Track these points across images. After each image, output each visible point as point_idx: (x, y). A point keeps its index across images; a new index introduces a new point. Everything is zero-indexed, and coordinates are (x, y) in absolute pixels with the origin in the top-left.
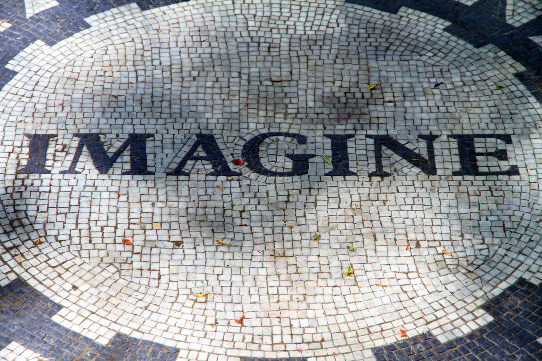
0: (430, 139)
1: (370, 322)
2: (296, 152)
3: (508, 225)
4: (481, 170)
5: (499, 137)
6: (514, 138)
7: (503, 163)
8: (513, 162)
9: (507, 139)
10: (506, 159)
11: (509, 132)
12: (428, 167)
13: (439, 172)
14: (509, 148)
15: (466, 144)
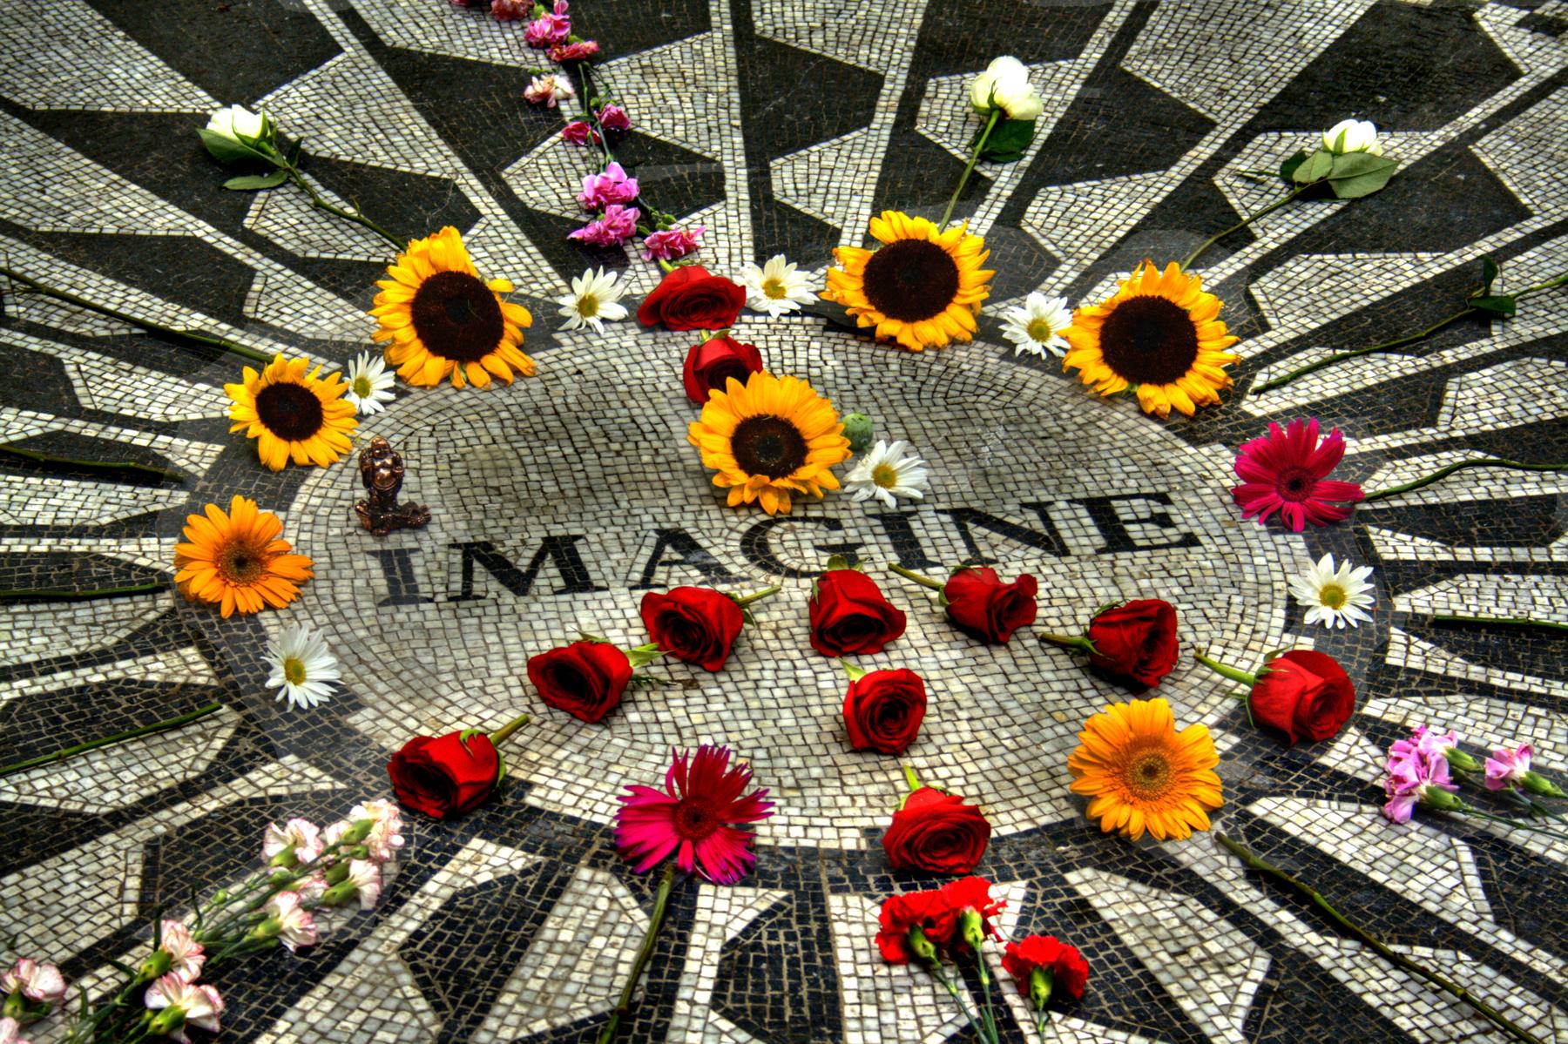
0: (1041, 508)
1: (1047, 761)
2: (832, 541)
3: (1211, 613)
4: (1139, 543)
5: (1147, 496)
6: (1173, 496)
7: (1169, 531)
8: (1184, 529)
9: (1163, 499)
10: (1171, 525)
11: (1162, 489)
12: (1052, 544)
13: (1076, 551)
14: (1171, 510)
15: (1101, 509)
